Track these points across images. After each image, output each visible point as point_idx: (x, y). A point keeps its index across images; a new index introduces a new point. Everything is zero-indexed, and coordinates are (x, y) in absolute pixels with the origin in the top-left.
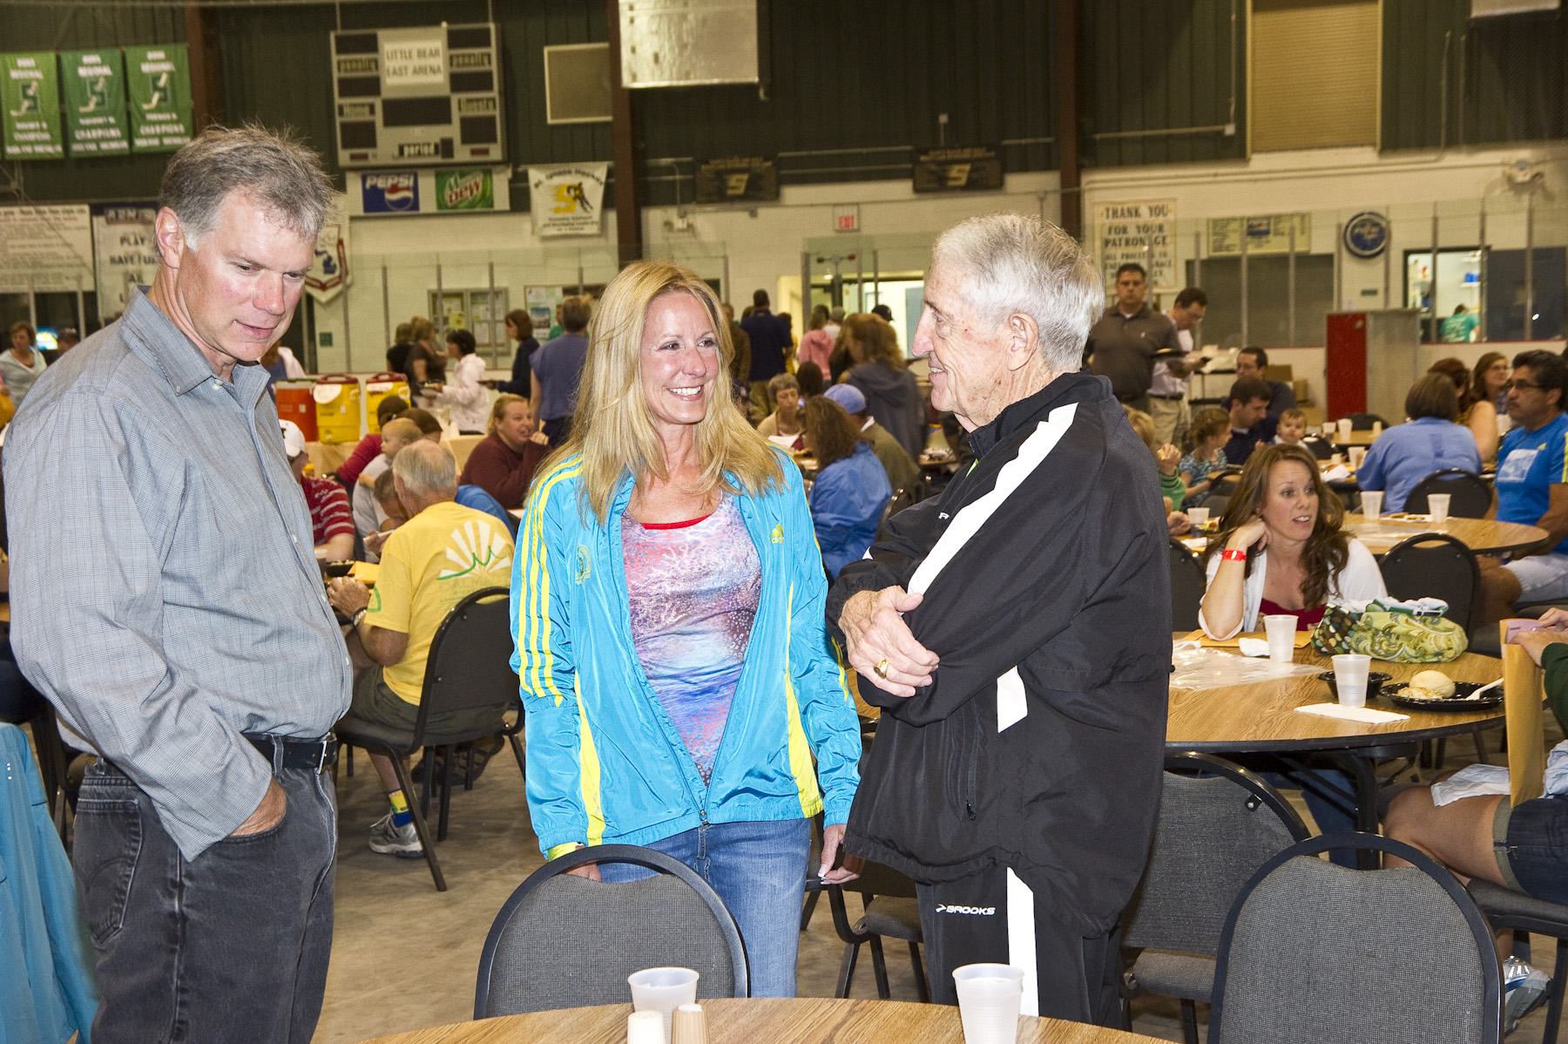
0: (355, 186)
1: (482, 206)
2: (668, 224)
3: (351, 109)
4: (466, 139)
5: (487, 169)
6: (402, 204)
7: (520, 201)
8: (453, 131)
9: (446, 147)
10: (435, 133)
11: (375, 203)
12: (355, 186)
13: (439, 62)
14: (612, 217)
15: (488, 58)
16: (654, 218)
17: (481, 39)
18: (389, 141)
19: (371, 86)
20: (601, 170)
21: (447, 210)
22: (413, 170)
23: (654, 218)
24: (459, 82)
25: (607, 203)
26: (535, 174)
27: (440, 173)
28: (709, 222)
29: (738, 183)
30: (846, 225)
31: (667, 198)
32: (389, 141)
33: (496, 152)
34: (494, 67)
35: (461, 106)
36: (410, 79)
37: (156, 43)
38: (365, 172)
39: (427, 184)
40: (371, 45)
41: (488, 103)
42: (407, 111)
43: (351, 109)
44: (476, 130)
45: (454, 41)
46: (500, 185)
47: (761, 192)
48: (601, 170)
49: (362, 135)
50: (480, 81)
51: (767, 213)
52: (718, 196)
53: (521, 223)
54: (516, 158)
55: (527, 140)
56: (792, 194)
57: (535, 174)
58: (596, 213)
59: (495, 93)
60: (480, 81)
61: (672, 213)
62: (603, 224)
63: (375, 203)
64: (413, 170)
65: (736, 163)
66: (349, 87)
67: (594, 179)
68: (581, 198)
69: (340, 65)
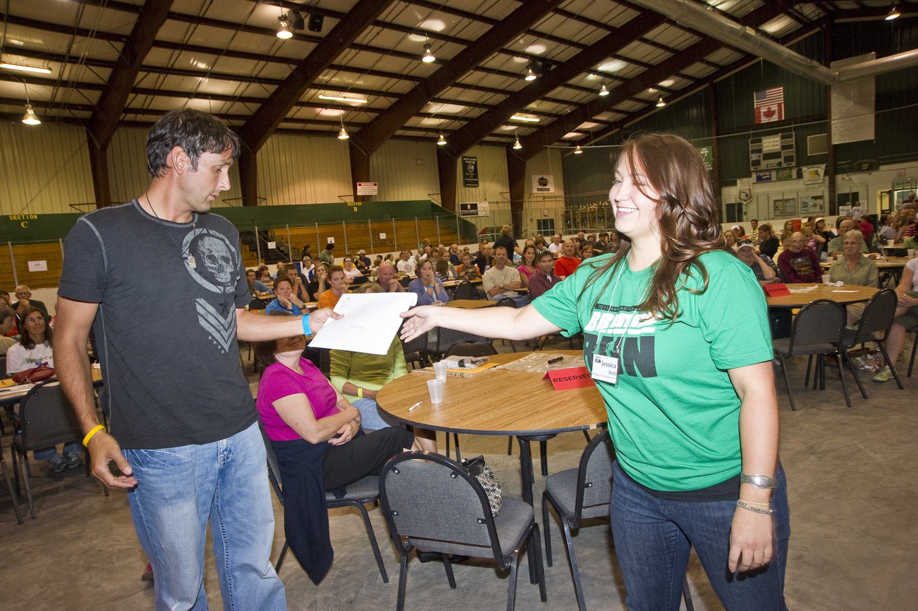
0: (754, 176)
1: (789, 177)
2: (843, 179)
3: (754, 157)
4: (785, 161)
5: (791, 168)
6: (767, 179)
7: (800, 176)
8: (782, 160)
9: (780, 164)
10: (777, 161)
11: (759, 179)
12: (754, 176)
13: (778, 143)
14: (827, 178)
15: (792, 141)
16: (839, 177)
17: (791, 136)
18: (764, 164)
19: (760, 151)
20: (824, 166)
21: (779, 179)
22: (770, 170)
23: (839, 177)
24: (783, 148)
25: (825, 174)
26: (804, 169)
27: (777, 170)
28: (856, 178)
29: (865, 166)
30: (900, 175)
31: (843, 171)
32: (764, 164)
33: (794, 164)
34: (794, 143)
35: (784, 154)
36: (770, 148)
37: (704, 147)
38: (757, 172)
39: (774, 174)
40: (760, 141)
41: (792, 152)
42: (768, 156)
43: (754, 157)
44: (788, 159)
45: (783, 138)
46: (794, 173)
47: (873, 168)
48: (824, 166)
49: (757, 163)
50: (790, 147)
51: (874, 173)
52: (859, 170)
53: (801, 181)
54: (799, 165)
55: (802, 159)
56: (883, 168)
57: (804, 169)
58: (822, 177)
59: (794, 149)
60: (790, 147)
61: (845, 176)
62: (824, 179)
63: (759, 179)
64: (770, 170)
65: (865, 161)
66: (753, 152)
67: (821, 169)
68: (817, 173)
69: (751, 147)
